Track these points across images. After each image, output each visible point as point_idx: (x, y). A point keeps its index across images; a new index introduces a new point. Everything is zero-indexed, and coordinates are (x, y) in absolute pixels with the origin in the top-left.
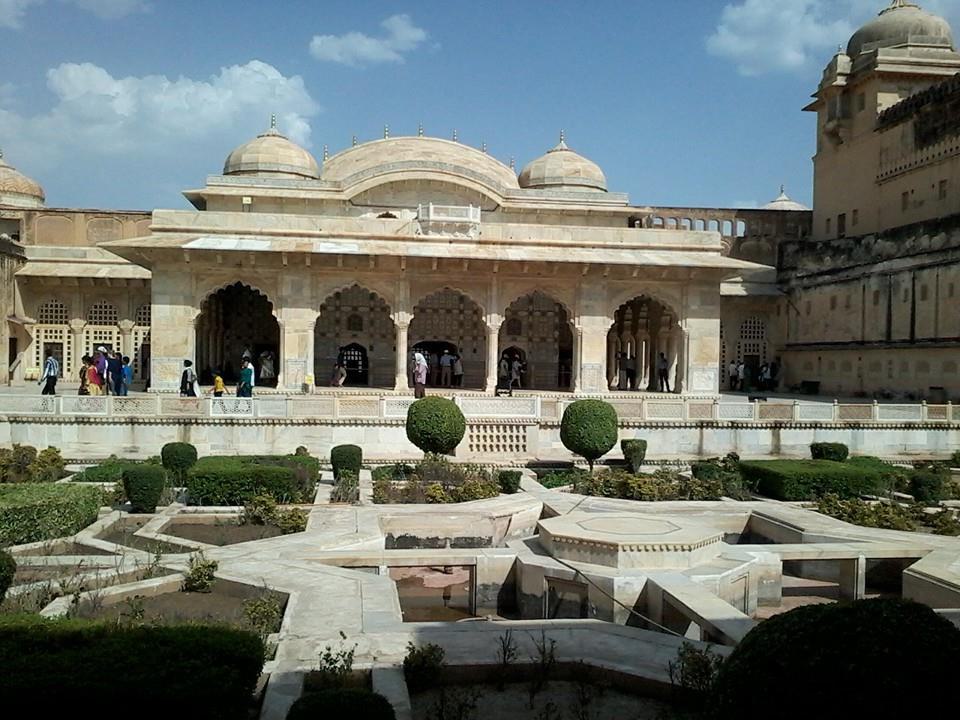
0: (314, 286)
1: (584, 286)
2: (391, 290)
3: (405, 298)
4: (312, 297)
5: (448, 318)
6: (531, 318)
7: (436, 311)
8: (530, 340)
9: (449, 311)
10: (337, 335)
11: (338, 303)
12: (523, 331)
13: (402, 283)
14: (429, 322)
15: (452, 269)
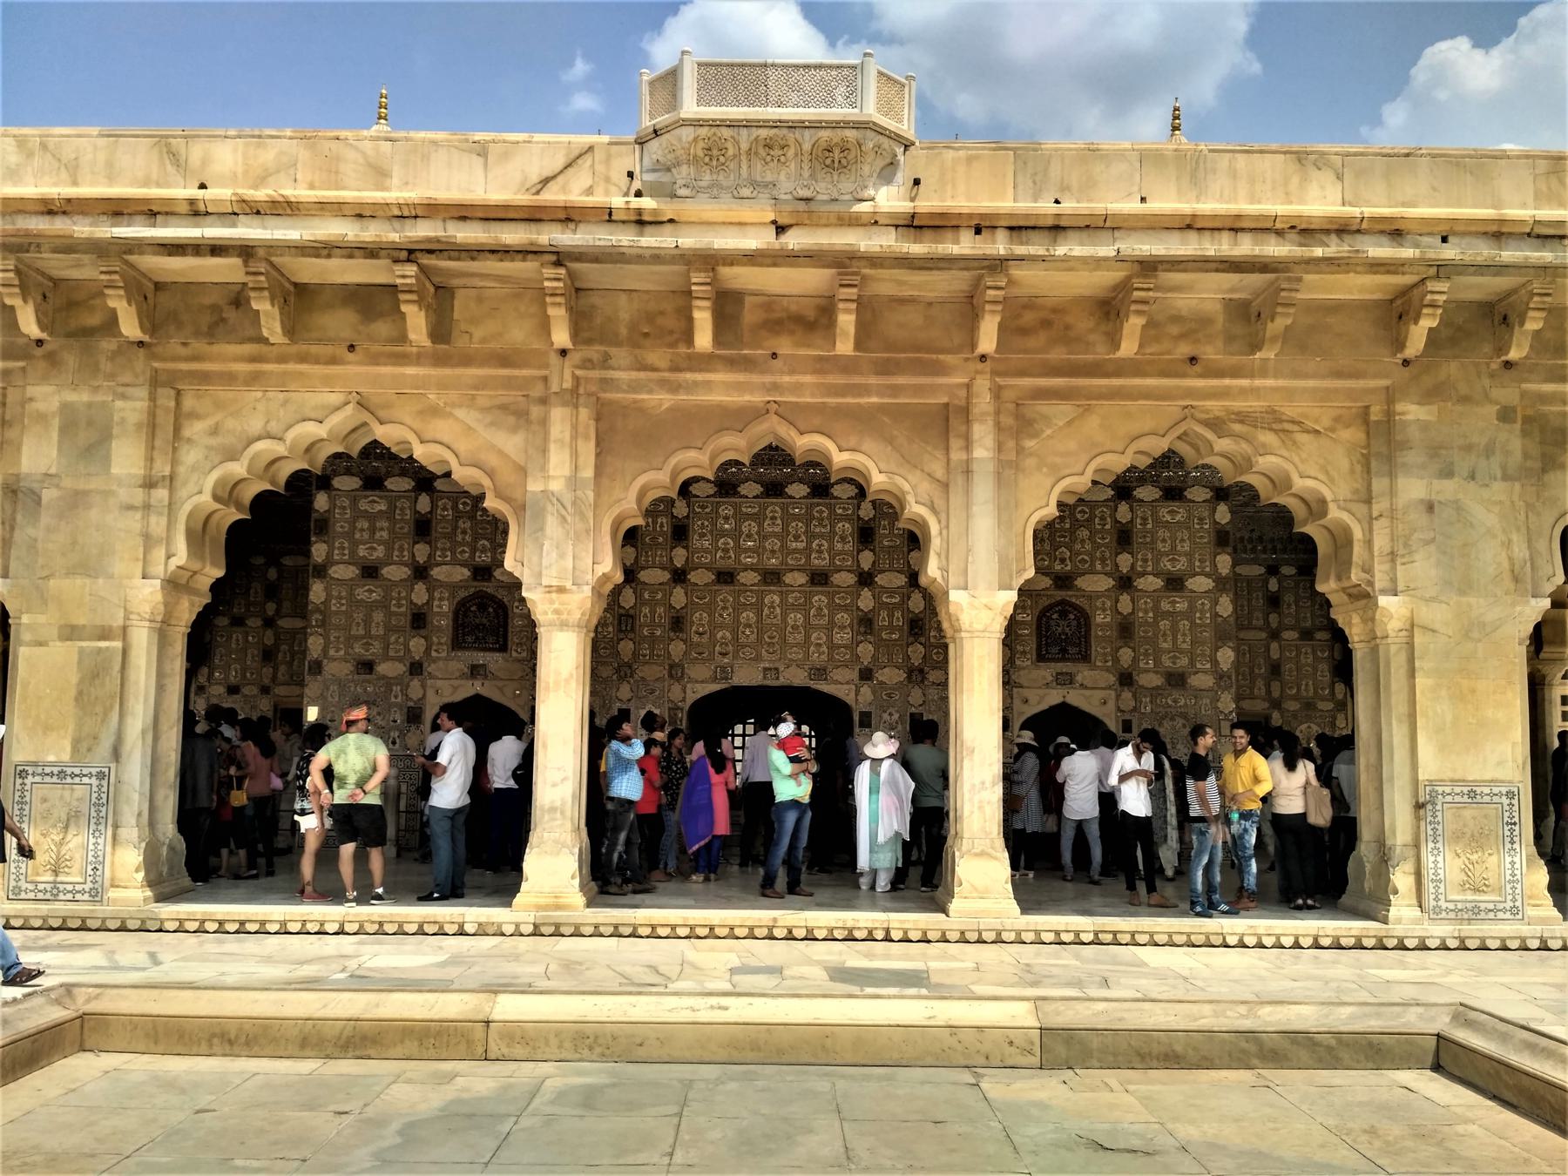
0: (166, 432)
1: (1412, 412)
2: (511, 443)
3: (573, 482)
4: (149, 484)
5: (820, 600)
6: (1125, 599)
7: (772, 577)
8: (1126, 679)
9: (819, 578)
10: (416, 669)
11: (421, 552)
12: (1096, 649)
13: (559, 417)
14: (748, 616)
15: (785, 346)
